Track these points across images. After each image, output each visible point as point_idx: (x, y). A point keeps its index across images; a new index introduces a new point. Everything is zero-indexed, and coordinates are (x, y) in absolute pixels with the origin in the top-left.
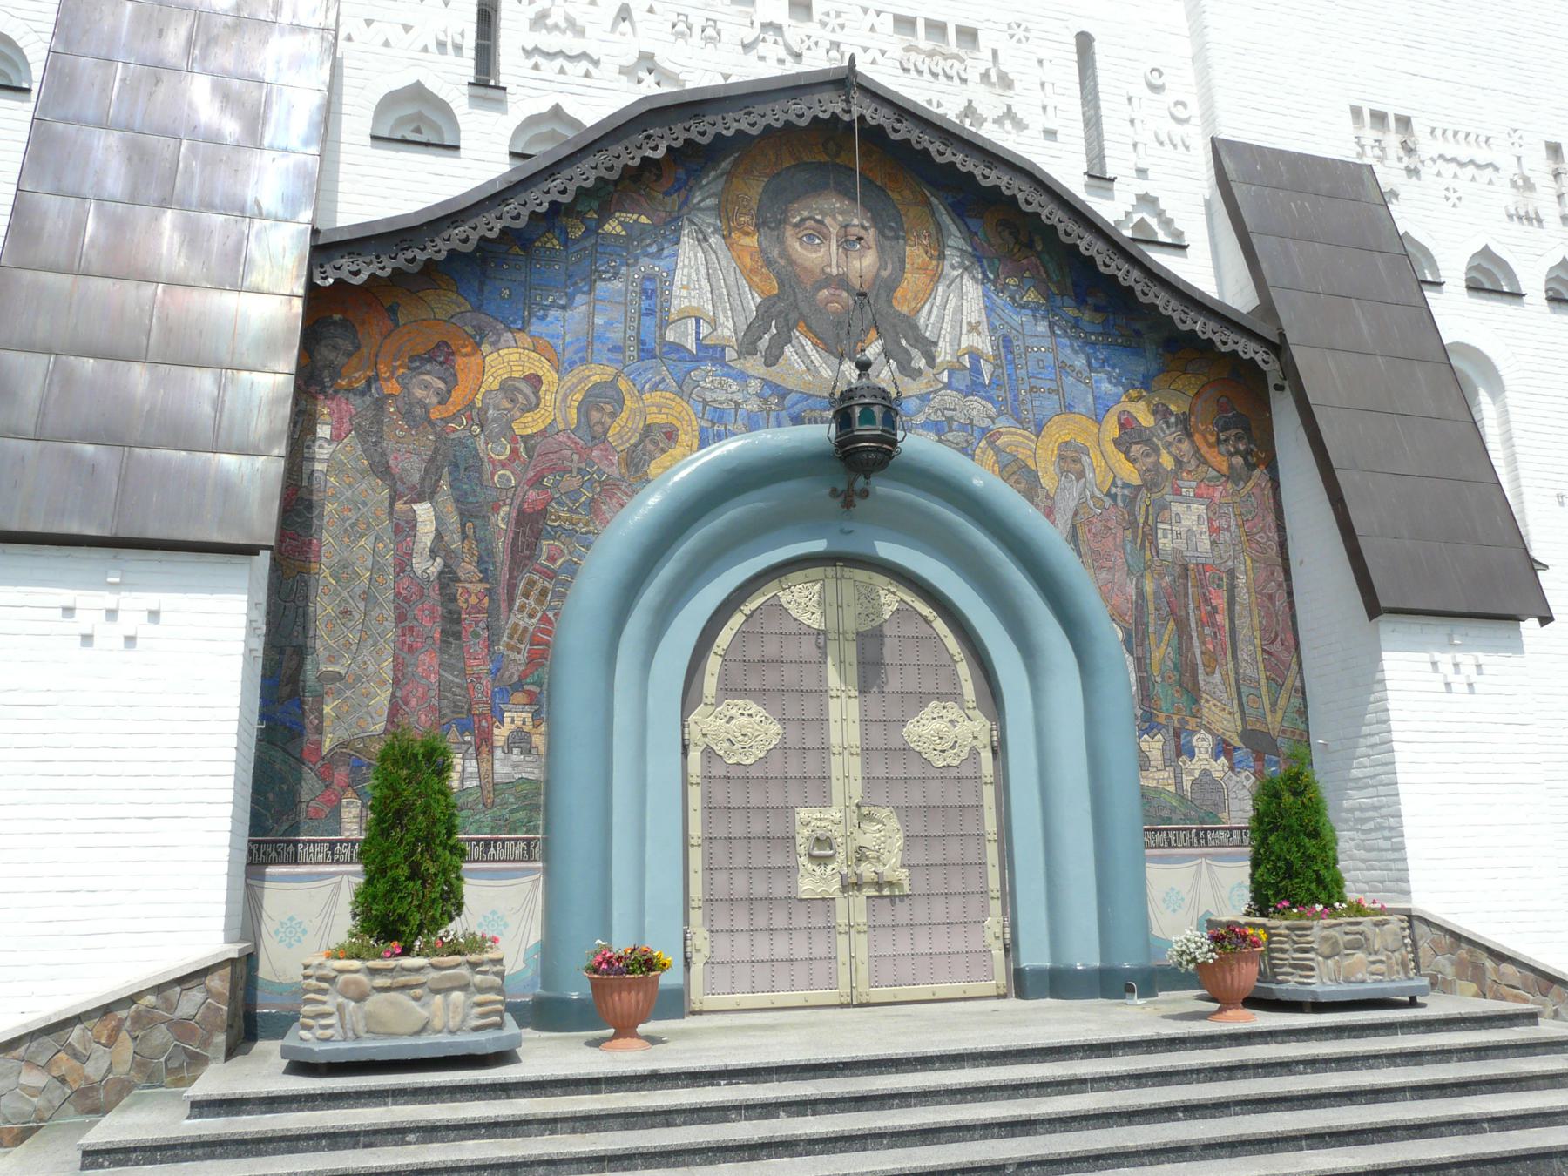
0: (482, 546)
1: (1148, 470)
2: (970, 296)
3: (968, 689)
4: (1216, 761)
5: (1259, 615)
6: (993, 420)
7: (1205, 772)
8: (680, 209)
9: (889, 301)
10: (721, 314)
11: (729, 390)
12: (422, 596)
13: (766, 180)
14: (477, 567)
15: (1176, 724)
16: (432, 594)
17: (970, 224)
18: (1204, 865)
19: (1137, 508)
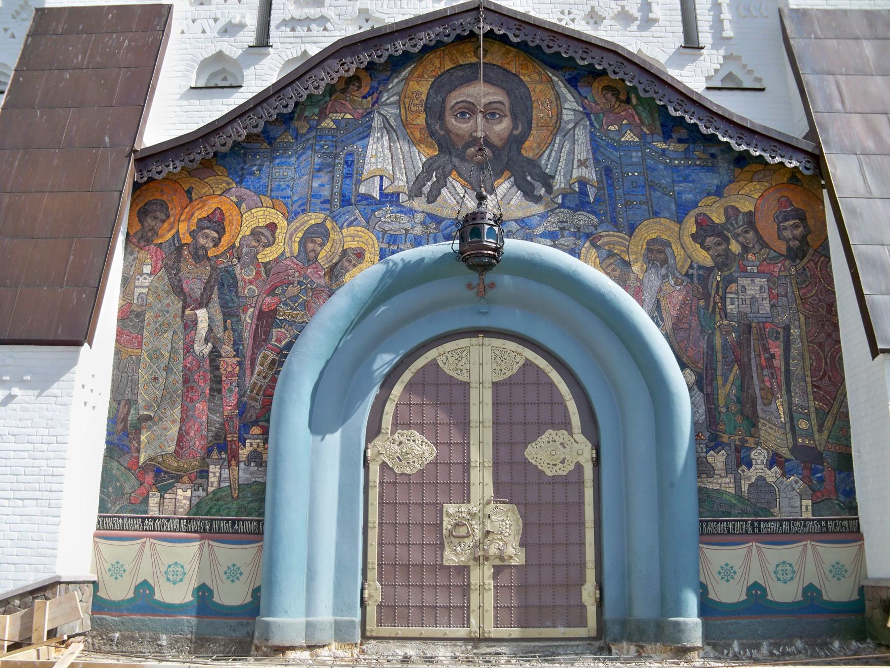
0: (236, 334)
1: (719, 255)
2: (580, 141)
3: (575, 419)
4: (770, 469)
5: (810, 358)
6: (596, 227)
7: (761, 478)
8: (373, 105)
9: (519, 151)
10: (398, 171)
11: (402, 222)
12: (199, 367)
13: (432, 80)
14: (233, 348)
15: (738, 443)
16: (205, 366)
17: (581, 91)
18: (754, 546)
19: (710, 284)
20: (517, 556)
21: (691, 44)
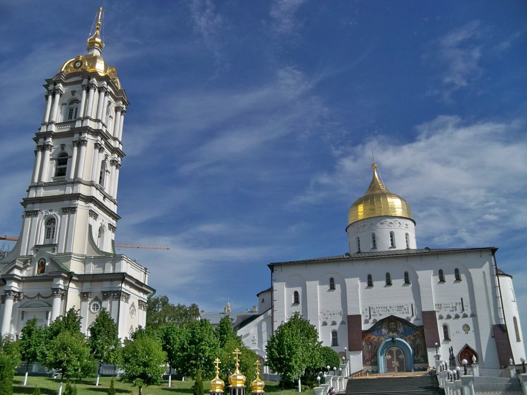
3: (403, 354)
20: (399, 366)
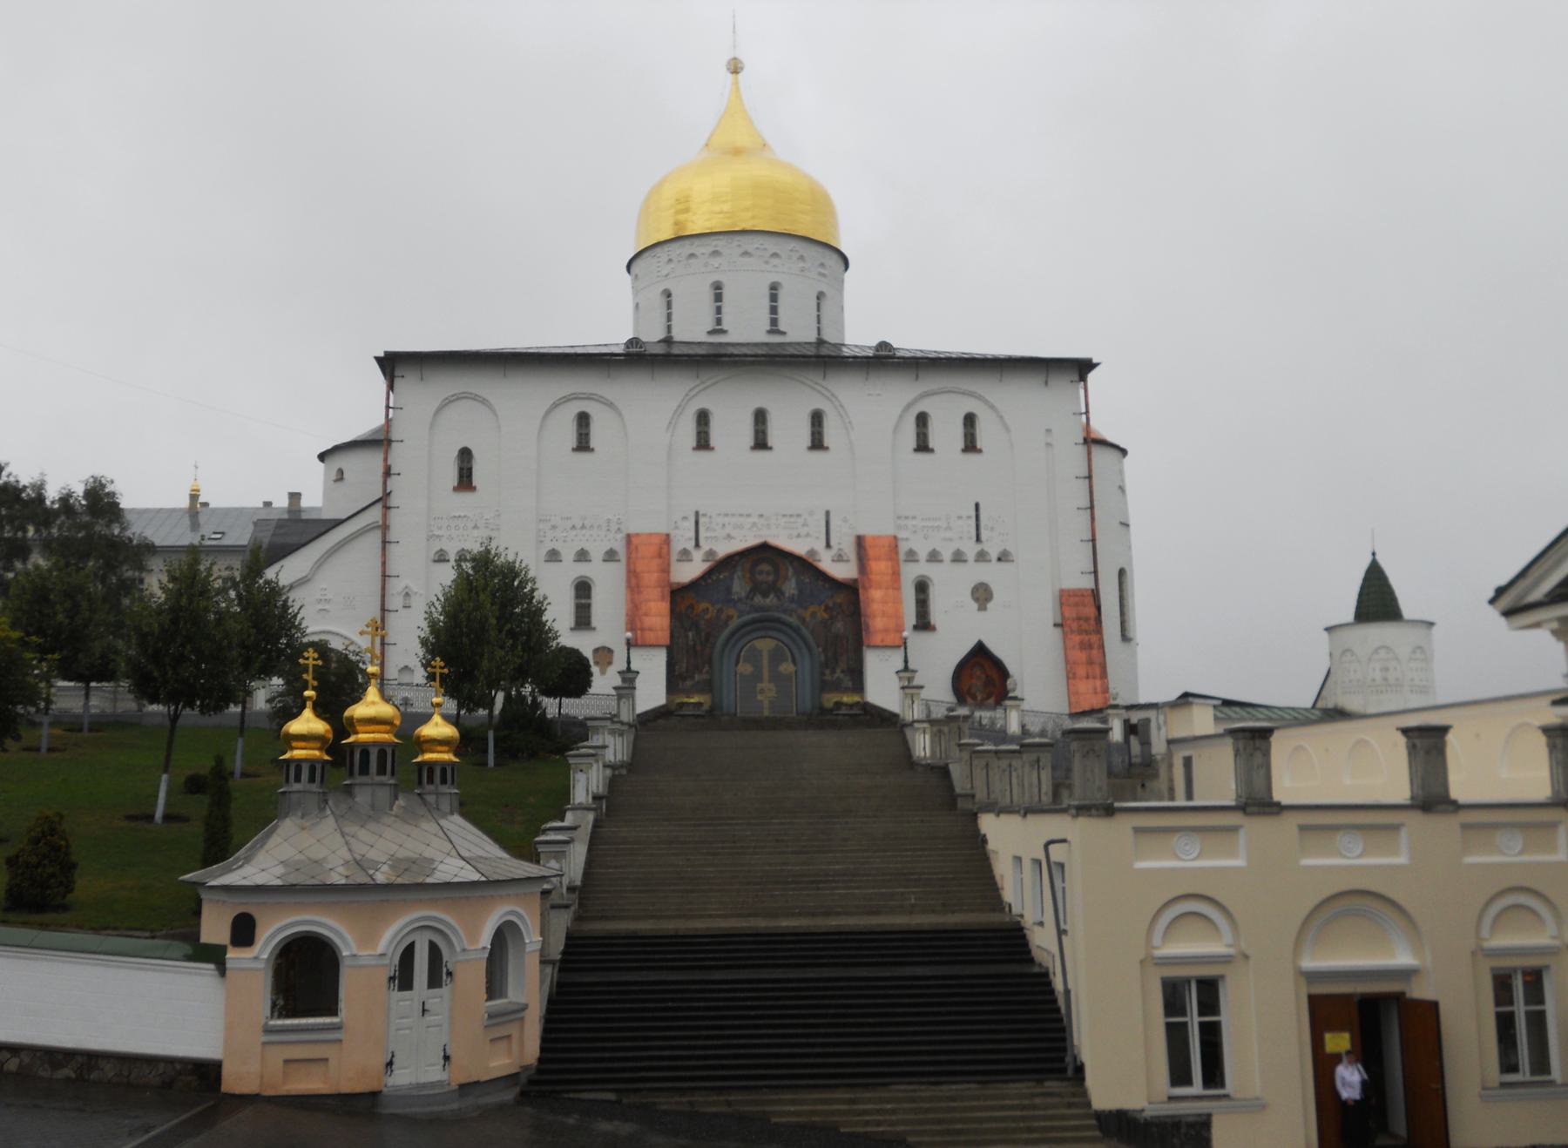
3: (790, 659)
21: (828, 545)
